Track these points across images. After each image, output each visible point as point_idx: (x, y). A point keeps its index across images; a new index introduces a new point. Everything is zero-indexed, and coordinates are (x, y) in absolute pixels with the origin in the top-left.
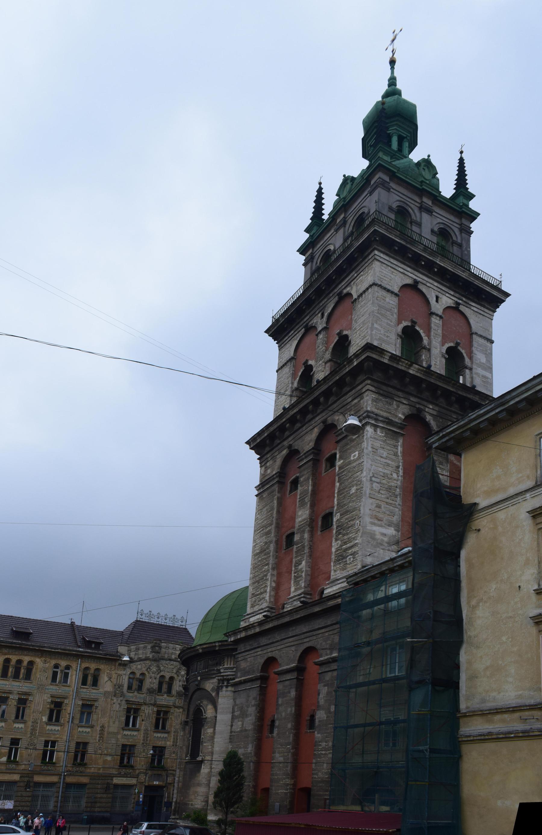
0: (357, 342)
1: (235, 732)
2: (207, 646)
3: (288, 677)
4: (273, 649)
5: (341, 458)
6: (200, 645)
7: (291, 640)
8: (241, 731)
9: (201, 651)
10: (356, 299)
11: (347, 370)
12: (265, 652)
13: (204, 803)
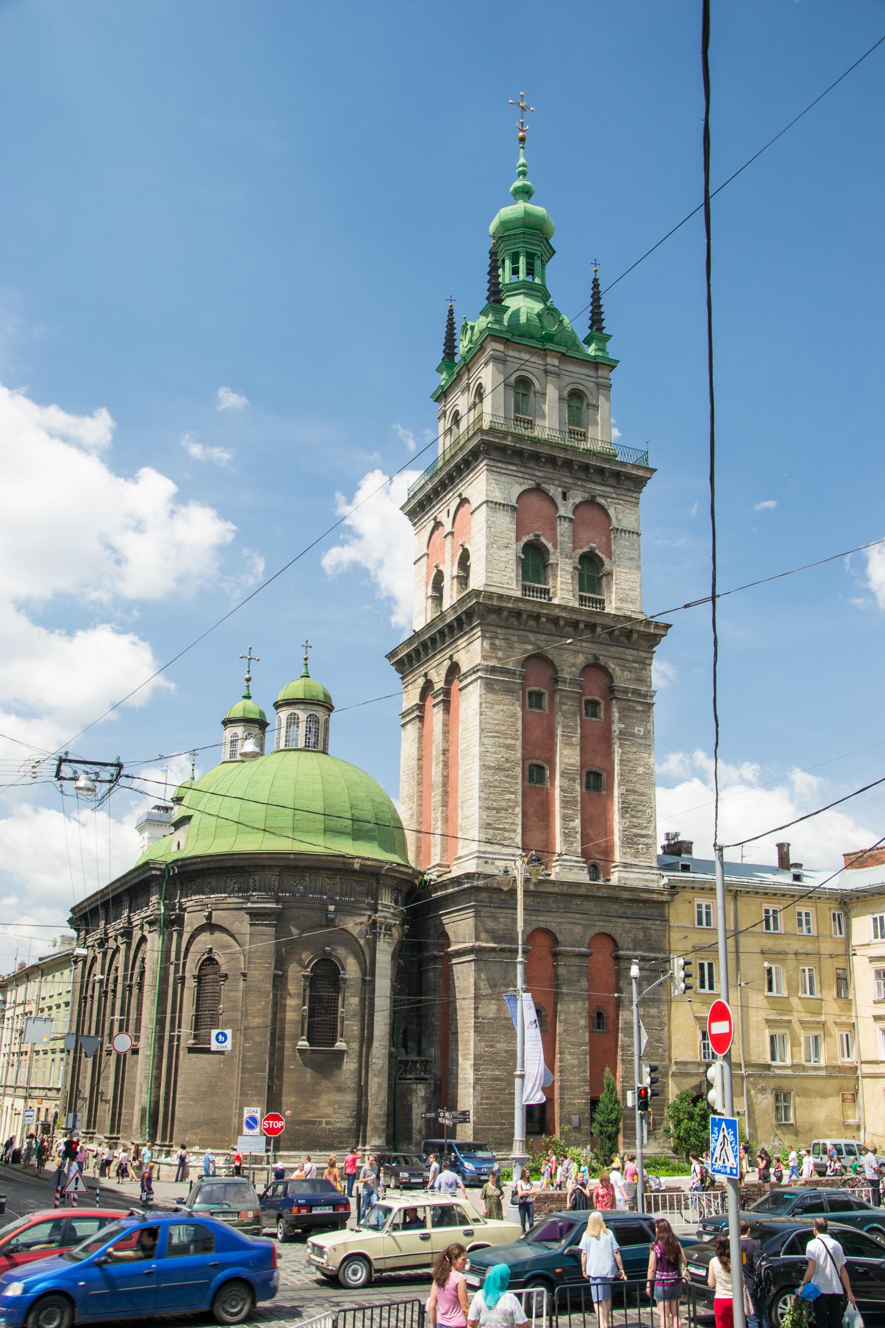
0: (624, 587)
1: (484, 1018)
2: (373, 863)
3: (575, 961)
4: (549, 919)
5: (620, 720)
6: (364, 859)
7: (578, 916)
8: (494, 1019)
9: (357, 866)
10: (617, 529)
11: (642, 629)
12: (534, 918)
13: (351, 1120)
